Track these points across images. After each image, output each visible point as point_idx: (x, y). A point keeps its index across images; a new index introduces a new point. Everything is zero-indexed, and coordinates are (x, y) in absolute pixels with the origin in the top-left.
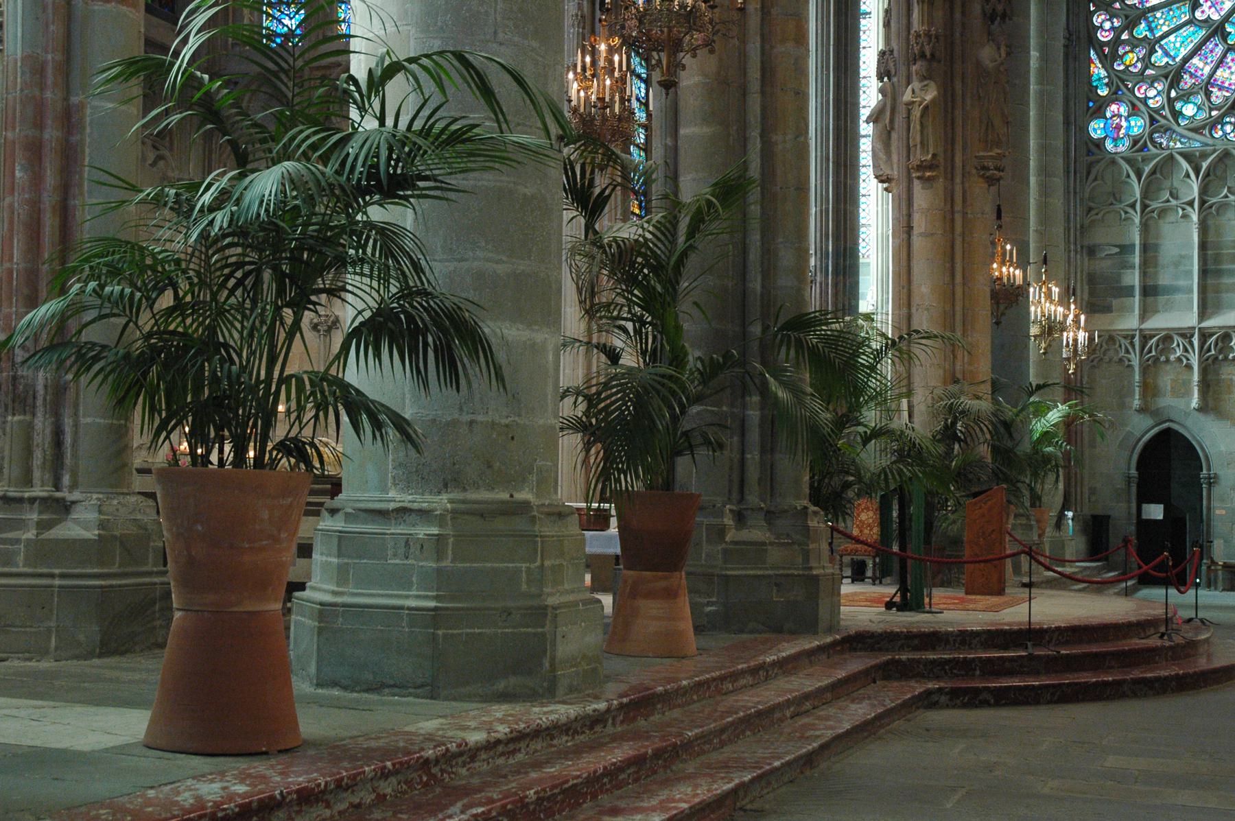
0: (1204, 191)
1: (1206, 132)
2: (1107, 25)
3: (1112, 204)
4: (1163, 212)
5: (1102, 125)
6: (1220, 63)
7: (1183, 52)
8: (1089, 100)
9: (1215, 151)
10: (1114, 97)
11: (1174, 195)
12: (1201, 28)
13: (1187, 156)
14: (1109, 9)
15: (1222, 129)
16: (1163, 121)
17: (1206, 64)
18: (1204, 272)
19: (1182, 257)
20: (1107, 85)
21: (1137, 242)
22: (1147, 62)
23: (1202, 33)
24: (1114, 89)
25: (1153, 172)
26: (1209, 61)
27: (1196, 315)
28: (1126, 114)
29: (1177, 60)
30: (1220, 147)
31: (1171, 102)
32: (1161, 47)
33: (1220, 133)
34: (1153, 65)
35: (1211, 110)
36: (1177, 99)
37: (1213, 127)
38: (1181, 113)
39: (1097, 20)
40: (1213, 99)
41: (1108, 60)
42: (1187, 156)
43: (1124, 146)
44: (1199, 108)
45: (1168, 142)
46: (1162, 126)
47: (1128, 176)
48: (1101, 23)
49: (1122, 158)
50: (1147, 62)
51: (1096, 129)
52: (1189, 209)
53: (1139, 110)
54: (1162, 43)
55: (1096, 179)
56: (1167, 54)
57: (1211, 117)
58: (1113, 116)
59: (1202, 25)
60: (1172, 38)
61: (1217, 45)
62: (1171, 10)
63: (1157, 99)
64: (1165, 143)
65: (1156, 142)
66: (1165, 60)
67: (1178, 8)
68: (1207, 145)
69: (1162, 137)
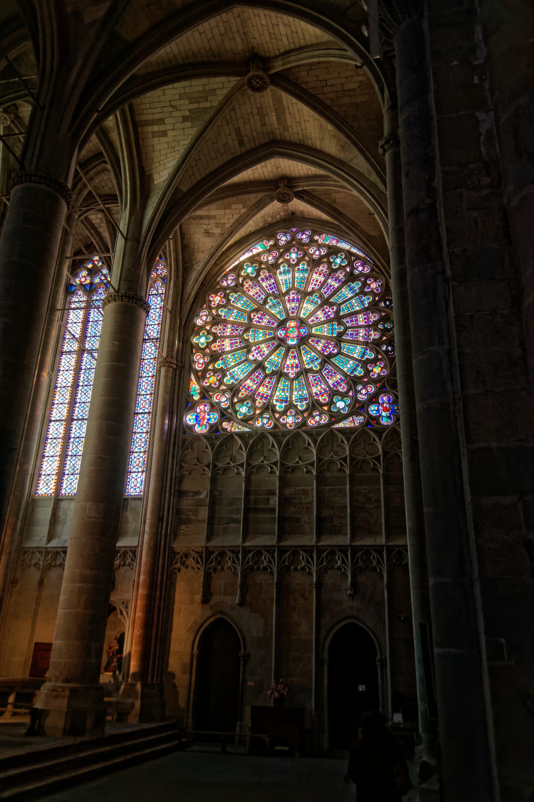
0: (250, 456)
2: (201, 361)
4: (226, 470)
5: (194, 417)
6: (261, 384)
7: (241, 377)
11: (233, 459)
16: (228, 415)
18: (247, 510)
19: (235, 499)
20: (199, 393)
22: (221, 382)
23: (254, 366)
25: (221, 445)
27: (241, 537)
28: (208, 411)
30: (260, 431)
31: (233, 404)
33: (261, 424)
40: (257, 404)
42: (241, 435)
50: (221, 382)
51: (190, 419)
52: (241, 469)
58: (201, 412)
60: (236, 369)
61: (260, 374)
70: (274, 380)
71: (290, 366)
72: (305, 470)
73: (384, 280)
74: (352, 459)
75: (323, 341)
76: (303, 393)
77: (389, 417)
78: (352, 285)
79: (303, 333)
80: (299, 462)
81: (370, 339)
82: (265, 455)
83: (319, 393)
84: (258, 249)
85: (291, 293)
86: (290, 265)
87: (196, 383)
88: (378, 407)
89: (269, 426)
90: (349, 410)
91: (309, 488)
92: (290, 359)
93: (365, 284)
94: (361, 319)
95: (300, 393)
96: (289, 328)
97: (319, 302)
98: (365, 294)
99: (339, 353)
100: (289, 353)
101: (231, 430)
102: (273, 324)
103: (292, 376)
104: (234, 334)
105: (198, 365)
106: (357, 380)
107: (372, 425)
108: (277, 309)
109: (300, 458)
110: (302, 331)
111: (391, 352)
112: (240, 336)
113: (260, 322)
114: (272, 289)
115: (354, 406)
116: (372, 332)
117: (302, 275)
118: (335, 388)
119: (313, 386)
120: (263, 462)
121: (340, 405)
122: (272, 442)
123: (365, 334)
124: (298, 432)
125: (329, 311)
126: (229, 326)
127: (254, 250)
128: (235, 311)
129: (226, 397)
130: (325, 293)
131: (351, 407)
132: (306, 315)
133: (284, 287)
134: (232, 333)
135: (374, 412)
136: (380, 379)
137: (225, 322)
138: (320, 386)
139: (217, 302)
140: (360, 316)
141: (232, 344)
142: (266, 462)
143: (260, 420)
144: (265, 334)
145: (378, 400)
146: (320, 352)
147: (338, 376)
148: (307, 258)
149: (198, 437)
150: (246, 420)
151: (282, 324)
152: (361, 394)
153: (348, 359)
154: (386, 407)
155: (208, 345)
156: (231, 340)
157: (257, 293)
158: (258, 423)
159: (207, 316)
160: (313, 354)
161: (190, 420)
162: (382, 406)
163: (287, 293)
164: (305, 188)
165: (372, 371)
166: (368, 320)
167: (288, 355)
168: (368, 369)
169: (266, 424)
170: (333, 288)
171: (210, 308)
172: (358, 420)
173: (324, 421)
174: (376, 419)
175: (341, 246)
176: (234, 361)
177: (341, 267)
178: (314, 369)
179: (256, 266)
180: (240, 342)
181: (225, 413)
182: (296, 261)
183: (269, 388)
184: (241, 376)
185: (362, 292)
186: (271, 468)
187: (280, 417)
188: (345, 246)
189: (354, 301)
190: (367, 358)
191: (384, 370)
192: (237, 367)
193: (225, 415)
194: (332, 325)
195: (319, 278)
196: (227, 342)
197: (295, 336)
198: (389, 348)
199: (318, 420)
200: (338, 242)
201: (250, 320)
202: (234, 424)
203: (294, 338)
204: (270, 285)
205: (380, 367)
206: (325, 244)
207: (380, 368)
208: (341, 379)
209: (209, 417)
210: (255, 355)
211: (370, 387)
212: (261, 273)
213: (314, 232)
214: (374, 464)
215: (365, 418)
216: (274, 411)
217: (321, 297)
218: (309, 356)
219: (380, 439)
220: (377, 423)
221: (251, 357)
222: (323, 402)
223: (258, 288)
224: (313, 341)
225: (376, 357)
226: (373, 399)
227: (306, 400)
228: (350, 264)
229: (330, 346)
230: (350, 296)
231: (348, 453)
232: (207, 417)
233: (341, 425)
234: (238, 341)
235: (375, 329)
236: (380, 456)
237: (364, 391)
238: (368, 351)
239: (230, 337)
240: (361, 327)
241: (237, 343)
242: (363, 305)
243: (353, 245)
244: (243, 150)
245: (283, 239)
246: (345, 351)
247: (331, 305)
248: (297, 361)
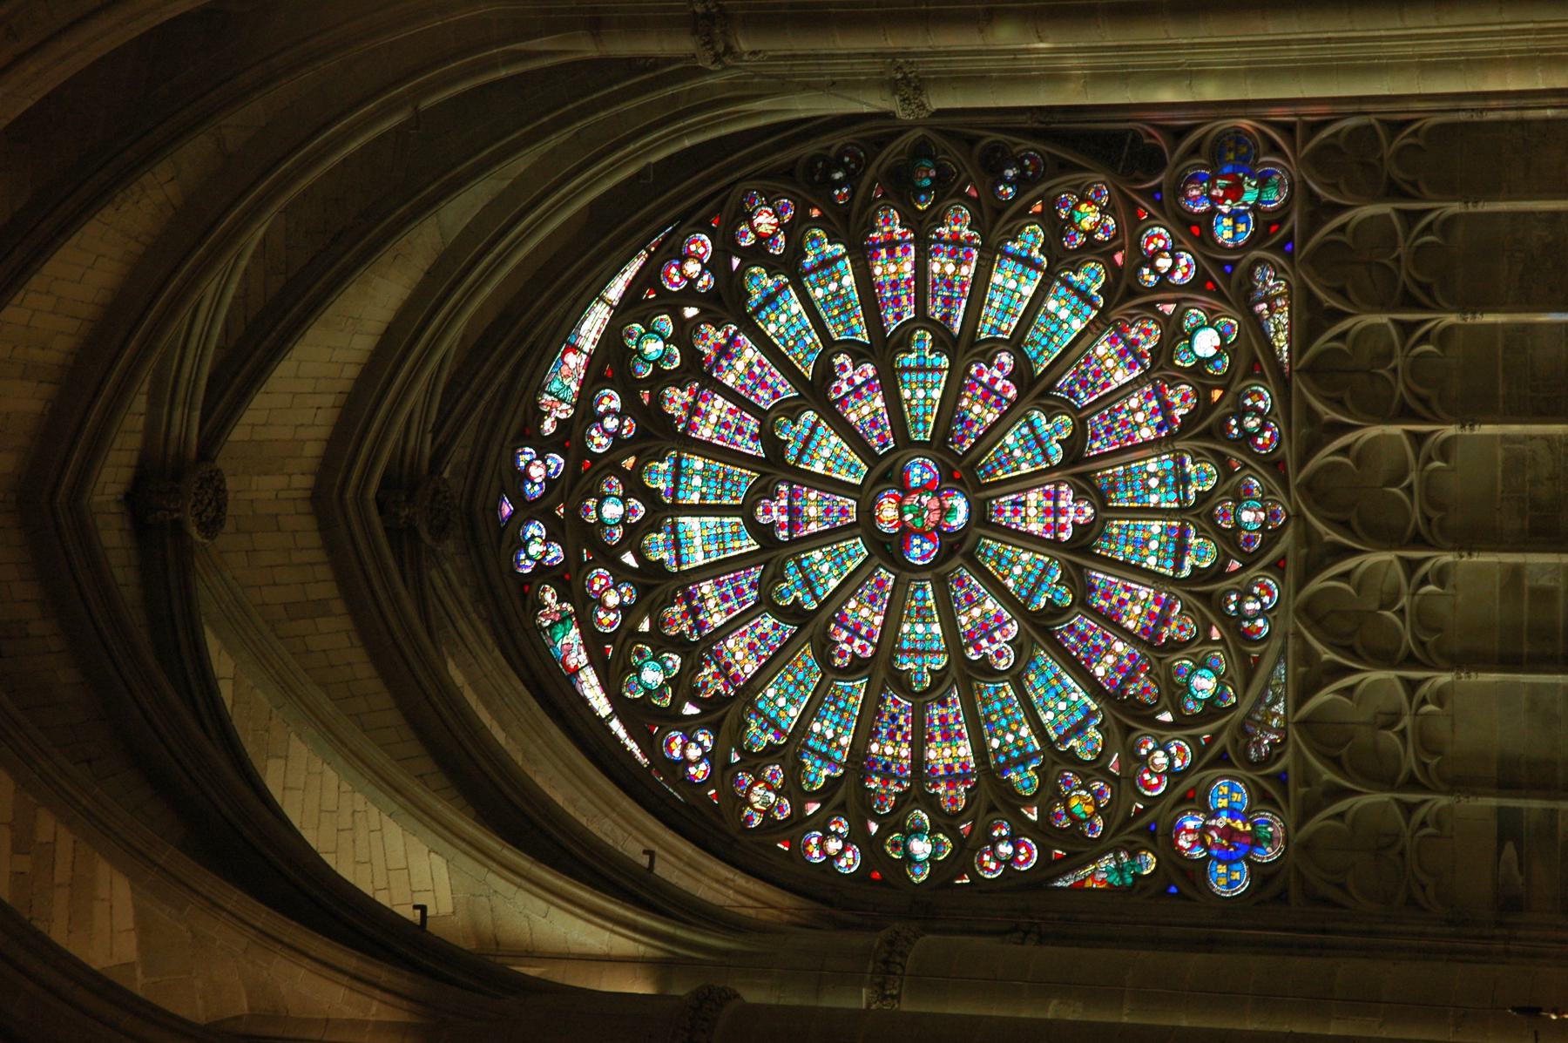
0: (1385, 659)
1: (1255, 651)
2: (1005, 849)
3: (1402, 854)
4: (1427, 744)
5: (1222, 869)
6: (1111, 620)
7: (1080, 695)
8: (1164, 893)
9: (1298, 634)
10: (1161, 837)
11: (1391, 719)
12: (1032, 659)
13: (1304, 690)
14: (970, 845)
15: (1252, 619)
16: (1224, 739)
17: (1109, 650)
20: (1133, 855)
21: (1493, 802)
22: (1091, 770)
24: (1143, 840)
25: (1336, 763)
26: (1103, 644)
28: (1201, 816)
29: (1094, 707)
30: (1291, 623)
31: (1182, 722)
32: (1064, 739)
33: (1260, 623)
34: (1100, 756)
35: (1208, 641)
36: (1177, 710)
37: (1247, 637)
38: (1209, 703)
39: (990, 869)
40: (1185, 635)
41: (1081, 849)
42: (1304, 690)
43: (1273, 825)
44: (1201, 664)
45: (1270, 730)
46: (1235, 742)
47: (1340, 816)
48: (999, 862)
49: (1298, 827)
50: (1091, 770)
51: (1231, 881)
53: (1193, 789)
54: (1054, 736)
55: (1341, 887)
56: (1079, 729)
57: (1222, 641)
58: (1201, 842)
59: (1026, 656)
60: (1046, 717)
61: (1072, 629)
62: (987, 717)
63: (1173, 750)
64: (1272, 737)
65: (1269, 754)
66: (1092, 731)
67: (985, 705)
68: (1283, 652)
69: (1259, 743)
70: (1099, 577)
71: (1050, 519)
72: (1437, 464)
73: (747, 185)
74: (1411, 303)
75: (965, 403)
76: (1155, 475)
77: (1263, 182)
78: (757, 297)
79: (927, 476)
80: (1406, 483)
81: (970, 238)
82: (1374, 606)
83: (1159, 419)
84: (570, 644)
85: (763, 519)
86: (652, 523)
87: (1092, 867)
88: (1223, 215)
89: (1270, 594)
90: (1230, 311)
91: (1500, 454)
92: (1024, 519)
93: (758, 253)
94: (892, 268)
95: (1154, 482)
97: (810, 416)
98: (796, 251)
99: (1016, 343)
100: (999, 525)
101: (1277, 731)
102: (881, 584)
103: (1089, 511)
104: (907, 729)
105: (1021, 863)
106: (1122, 286)
107: (1289, 237)
108: (825, 568)
109: (1396, 482)
110: (916, 476)
111: (1024, 169)
112: (921, 701)
113: (870, 634)
114: (739, 592)
115: (1220, 295)
116: (944, 230)
117: (697, 481)
118: (1147, 361)
119: (1131, 438)
121: (1206, 343)
122: (1332, 578)
123: (951, 255)
124: (1298, 487)
125: (850, 381)
126: (874, 748)
127: (572, 661)
128: (816, 727)
129: (1150, 753)
130: (776, 394)
131: (1216, 304)
132: (859, 461)
133: (737, 544)
134: (904, 738)
135: (1242, 228)
136: (1124, 209)
137: (860, 761)
138: (1133, 412)
139: (772, 797)
140: (878, 271)
141: (946, 737)
142: (1404, 601)
143: (1246, 624)
144: (923, 615)
145: (1199, 214)
146: (1003, 415)
147: (1101, 350)
148: (629, 463)
149: (1300, 849)
150: (1245, 671)
151: (887, 549)
152: (1172, 270)
153: (1041, 318)
154: (1226, 188)
155: (944, 822)
156: (932, 738)
157: (752, 646)
158: (1261, 629)
159: (827, 834)
160: (1009, 439)
161: (1230, 884)
162: (1222, 201)
163: (763, 534)
164: (430, 427)
165: (1089, 234)
166: (898, 243)
167: (1008, 528)
168: (1081, 247)
169: (1263, 605)
170: (760, 364)
171: (799, 823)
172: (1270, 281)
173: (1261, 397)
174: (1267, 224)
175: (594, 335)
176: (1014, 727)
177: (684, 335)
178: (1064, 435)
179: (640, 653)
180: (943, 704)
181: (1215, 749)
182: (633, 502)
183: (1127, 596)
184: (1074, 697)
185: (791, 267)
186: (1425, 581)
187: (1242, 551)
188: (593, 325)
189: (819, 293)
190: (1041, 251)
191: (1091, 193)
192: (1040, 712)
193: (1223, 752)
194: (909, 370)
195: (713, 419)
196: (936, 754)
197: (935, 504)
198: (1010, 173)
199: (1258, 420)
200: (575, 349)
201: (858, 666)
202: (1258, 718)
203: (942, 507)
204: (725, 598)
205: (1076, 207)
206: (579, 395)
207: (1083, 207)
208: (1113, 341)
209: (1224, 815)
210: (995, 647)
211: (1150, 240)
212: (672, 632)
213: (529, 434)
214: (1428, 229)
215: (1259, 261)
216: (1218, 572)
217: (791, 410)
218: (1017, 453)
219: (1339, 209)
220: (1281, 222)
222: (1192, 402)
223: (730, 643)
224: (962, 438)
225: (1040, 218)
226: (1195, 231)
227: (1182, 463)
228: (672, 304)
229: (985, 378)
230: (796, 307)
231: (1383, 319)
232: (1223, 820)
233: (1281, 342)
234: (936, 711)
235: (935, 218)
236: (1398, 211)
237: (1164, 263)
238: (1017, 246)
239: (919, 743)
240: (921, 267)
241: (943, 719)
242: (836, 259)
243: (597, 294)
244: (338, 606)
245: (538, 546)
246: (1009, 325)
247: (826, 373)
248: (1033, 497)
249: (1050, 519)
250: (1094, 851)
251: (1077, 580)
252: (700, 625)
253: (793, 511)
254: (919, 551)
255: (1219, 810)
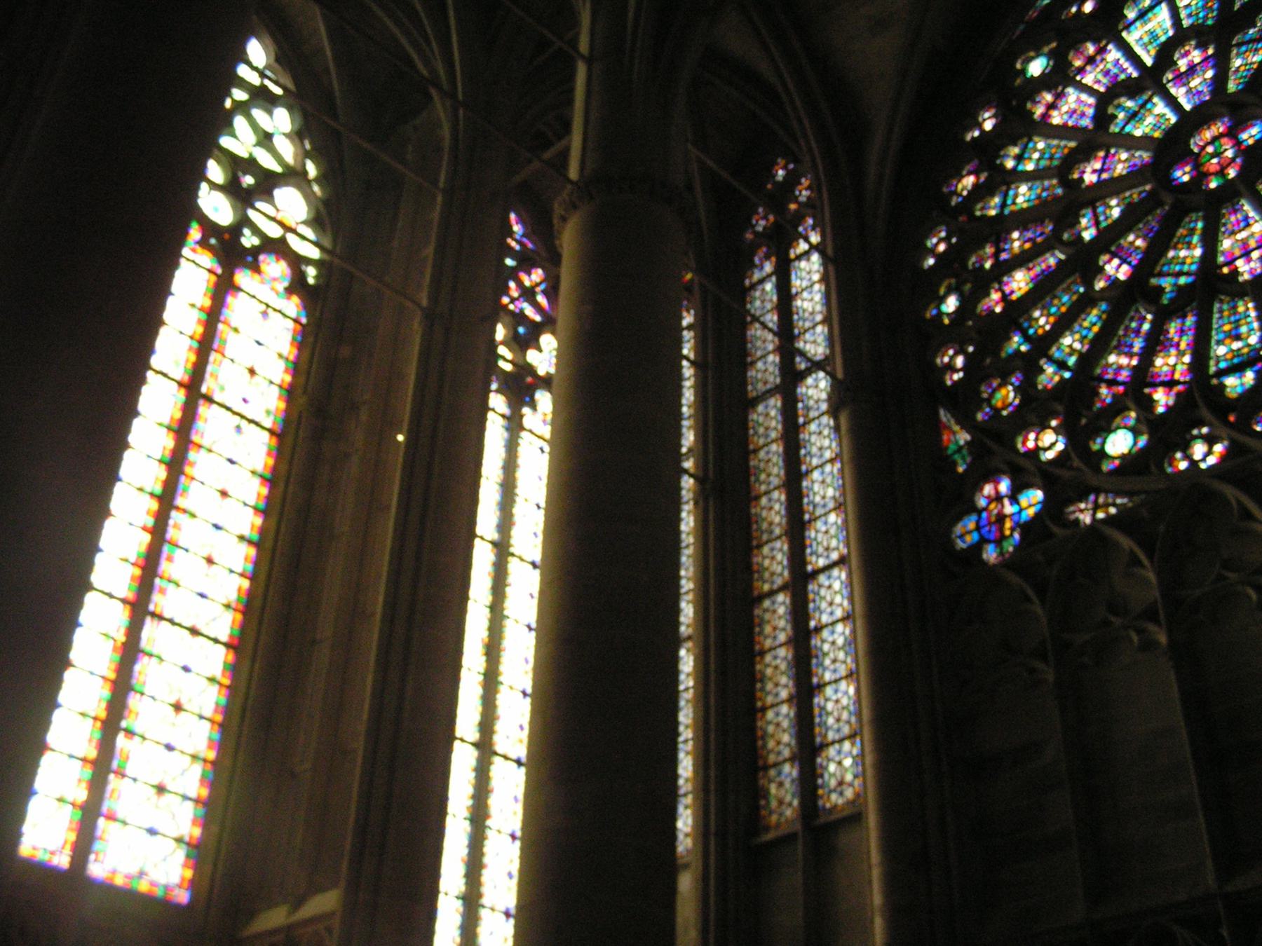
2: (959, 361)
6: (1156, 342)
44: (1136, 432)
52: (1152, 627)
62: (1055, 297)
96: (1203, 148)
120: (1226, 578)
221: (1100, 285)
232: (1009, 509)
249: (1237, 252)
250: (967, 422)
251: (1185, 300)
252: (1081, 70)
253: (1192, 69)
254: (1183, 175)
255: (1018, 503)
